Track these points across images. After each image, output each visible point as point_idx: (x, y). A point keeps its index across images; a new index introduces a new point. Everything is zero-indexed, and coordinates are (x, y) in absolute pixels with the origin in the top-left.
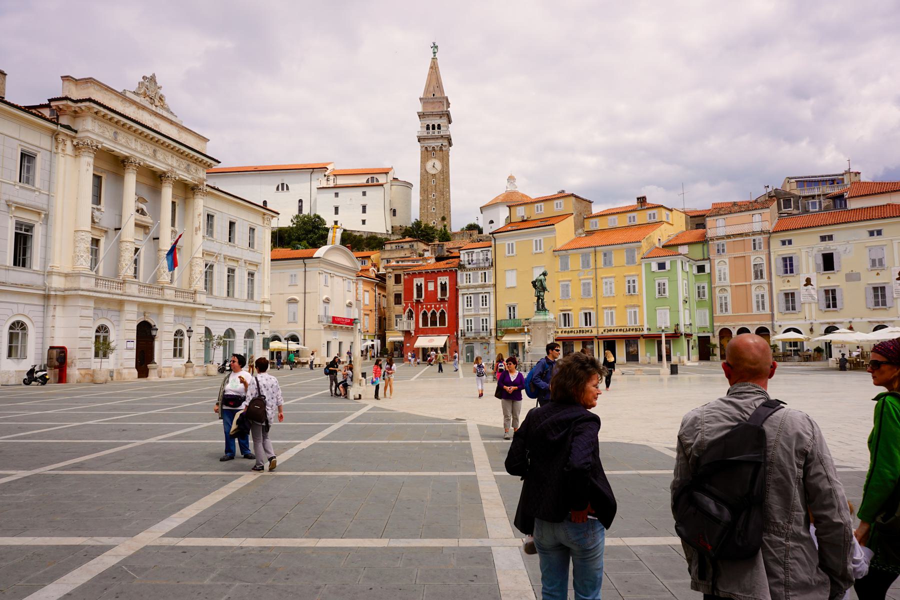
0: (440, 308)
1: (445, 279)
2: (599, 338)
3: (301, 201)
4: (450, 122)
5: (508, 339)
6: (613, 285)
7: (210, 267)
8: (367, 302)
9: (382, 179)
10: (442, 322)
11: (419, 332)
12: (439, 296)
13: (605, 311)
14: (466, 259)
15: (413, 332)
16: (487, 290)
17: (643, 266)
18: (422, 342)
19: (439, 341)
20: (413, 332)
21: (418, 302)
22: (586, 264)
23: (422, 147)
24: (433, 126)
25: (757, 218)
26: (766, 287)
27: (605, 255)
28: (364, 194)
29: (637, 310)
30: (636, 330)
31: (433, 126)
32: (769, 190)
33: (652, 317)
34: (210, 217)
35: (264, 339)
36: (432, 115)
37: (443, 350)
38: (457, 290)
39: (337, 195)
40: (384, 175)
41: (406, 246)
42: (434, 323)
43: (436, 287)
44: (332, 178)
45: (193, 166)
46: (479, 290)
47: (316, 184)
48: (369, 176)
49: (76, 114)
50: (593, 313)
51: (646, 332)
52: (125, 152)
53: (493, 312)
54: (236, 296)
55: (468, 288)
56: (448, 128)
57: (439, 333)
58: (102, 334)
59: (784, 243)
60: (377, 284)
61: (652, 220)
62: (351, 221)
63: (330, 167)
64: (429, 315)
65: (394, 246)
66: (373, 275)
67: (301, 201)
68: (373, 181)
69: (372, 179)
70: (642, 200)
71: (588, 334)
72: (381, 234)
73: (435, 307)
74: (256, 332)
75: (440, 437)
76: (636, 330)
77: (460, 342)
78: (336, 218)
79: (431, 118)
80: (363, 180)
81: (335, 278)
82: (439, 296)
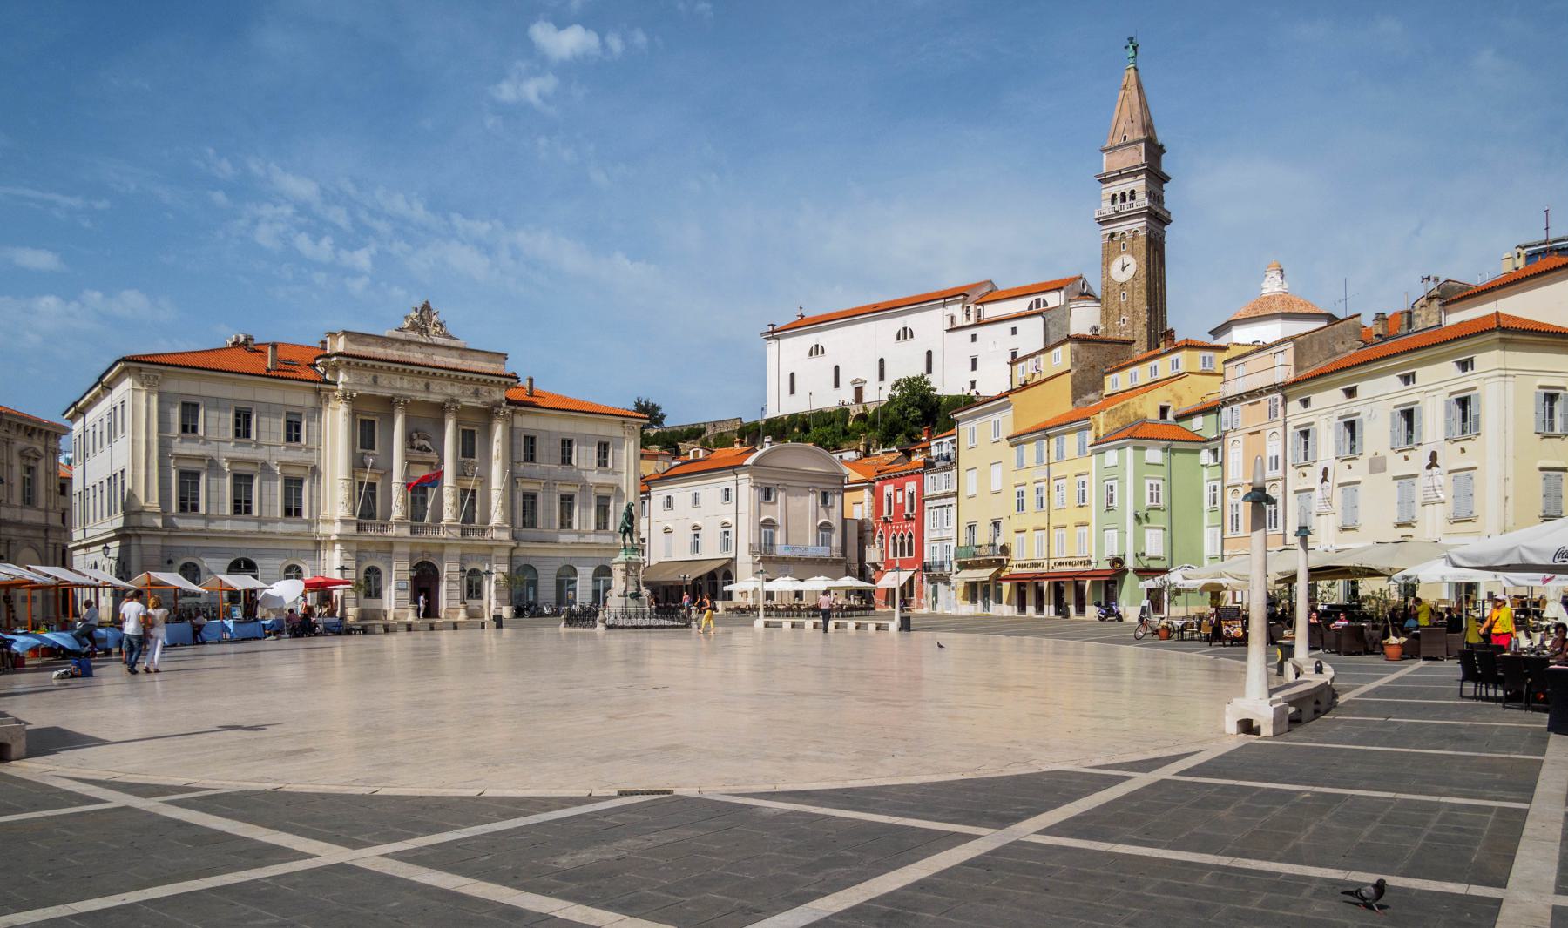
1: (911, 486)
3: (929, 353)
4: (1165, 179)
7: (530, 500)
9: (1053, 299)
10: (910, 553)
12: (907, 511)
20: (882, 567)
22: (1039, 460)
24: (1123, 195)
25: (1280, 359)
26: (1280, 484)
28: (1014, 331)
32: (1432, 285)
34: (530, 441)
36: (1121, 175)
39: (974, 338)
40: (1056, 294)
42: (902, 554)
45: (484, 389)
47: (947, 327)
48: (1033, 298)
49: (335, 369)
52: (387, 393)
58: (372, 577)
59: (1306, 403)
61: (1176, 371)
64: (898, 540)
67: (929, 353)
68: (1038, 306)
71: (1040, 570)
75: (1453, 788)
78: (973, 376)
82: (907, 511)
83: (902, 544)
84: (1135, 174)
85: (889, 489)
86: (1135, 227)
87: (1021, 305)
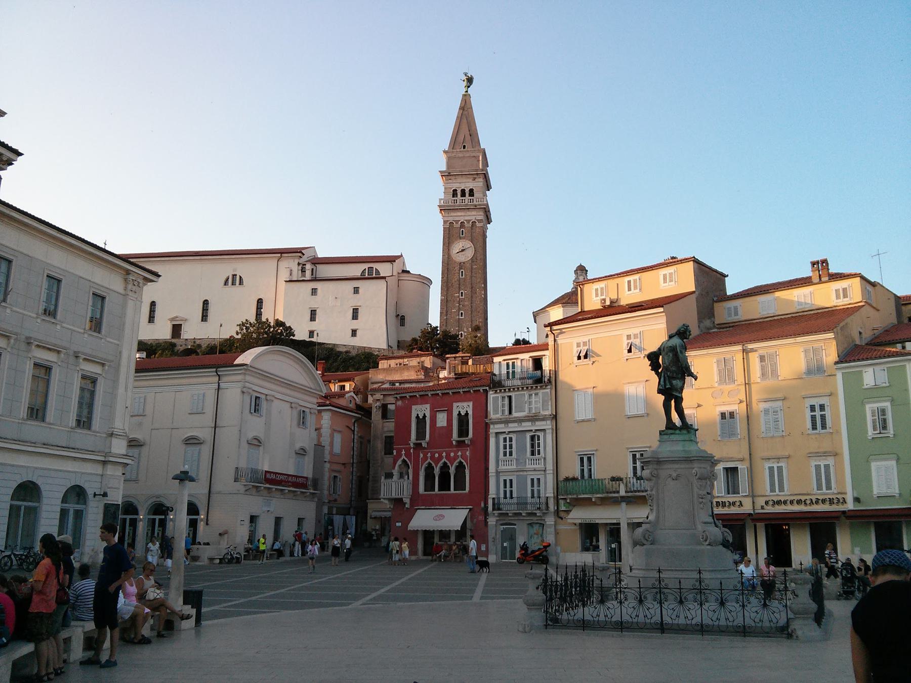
0: (456, 457)
1: (465, 407)
2: (755, 518)
3: (260, 302)
4: (488, 187)
5: (580, 515)
6: (780, 415)
8: (337, 449)
9: (384, 269)
10: (460, 485)
11: (418, 502)
13: (767, 465)
14: (504, 371)
15: (407, 501)
16: (540, 425)
17: (839, 376)
18: (424, 520)
19: (453, 519)
20: (407, 501)
21: (418, 446)
23: (445, 222)
24: (463, 192)
27: (762, 358)
28: (356, 290)
29: (830, 461)
30: (831, 502)
31: (463, 192)
33: (861, 476)
35: (107, 507)
37: (461, 534)
38: (487, 426)
39: (314, 292)
40: (388, 265)
41: (414, 362)
42: (444, 485)
43: (450, 420)
44: (308, 267)
46: (527, 426)
47: (284, 275)
48: (366, 266)
50: (742, 467)
51: (850, 506)
53: (550, 466)
54: (50, 415)
55: (506, 422)
56: (485, 195)
57: (454, 503)
60: (357, 420)
62: (333, 331)
63: (308, 254)
64: (437, 471)
65: (393, 363)
66: (352, 406)
67: (260, 302)
69: (370, 268)
70: (821, 265)
71: (734, 510)
72: (379, 350)
73: (448, 456)
74: (90, 492)
76: (831, 502)
77: (492, 521)
78: (313, 326)
79: (459, 179)
80: (356, 270)
81: (276, 402)
83: (445, 475)
84: (474, 176)
85: (421, 410)
86: (473, 219)
87: (356, 270)
